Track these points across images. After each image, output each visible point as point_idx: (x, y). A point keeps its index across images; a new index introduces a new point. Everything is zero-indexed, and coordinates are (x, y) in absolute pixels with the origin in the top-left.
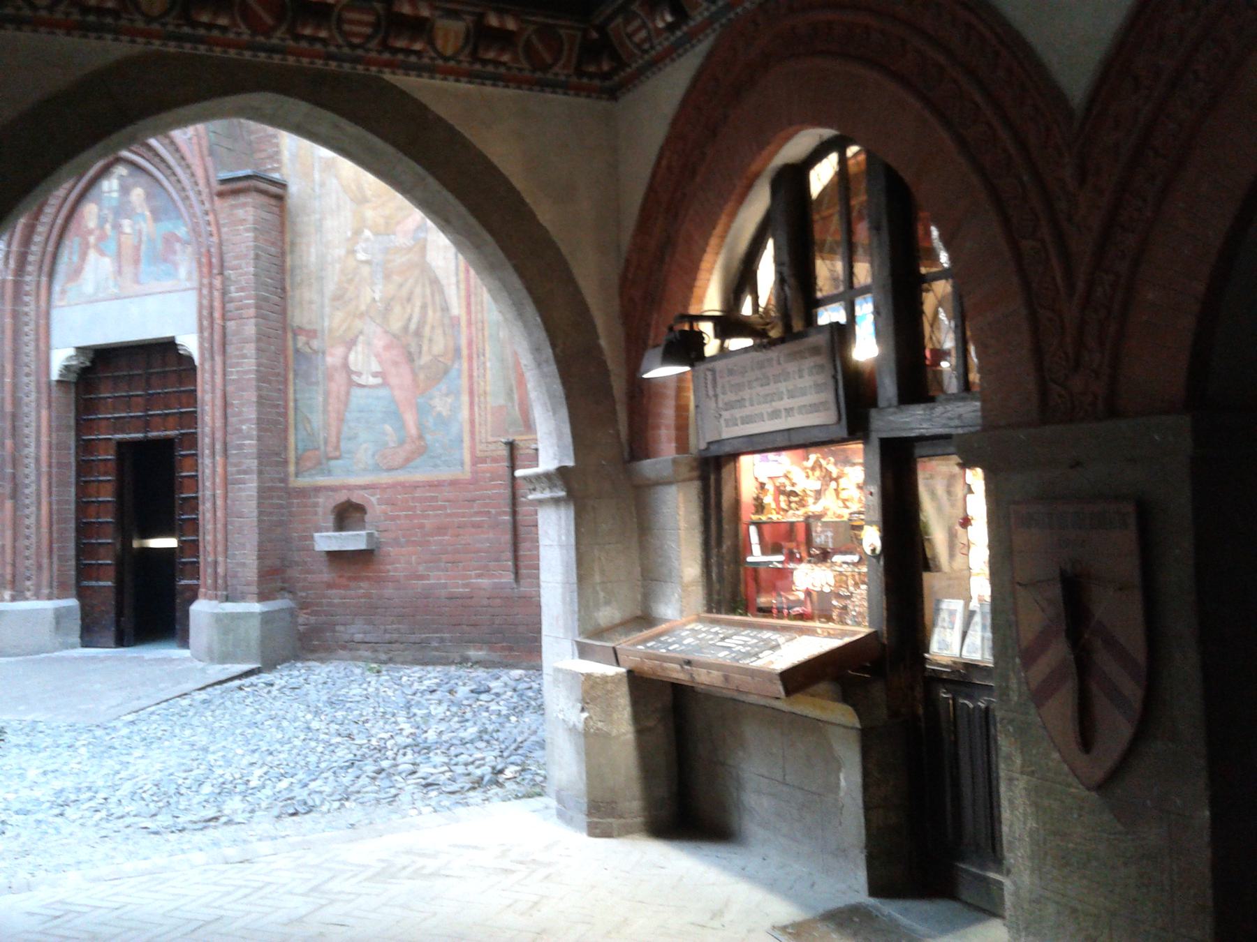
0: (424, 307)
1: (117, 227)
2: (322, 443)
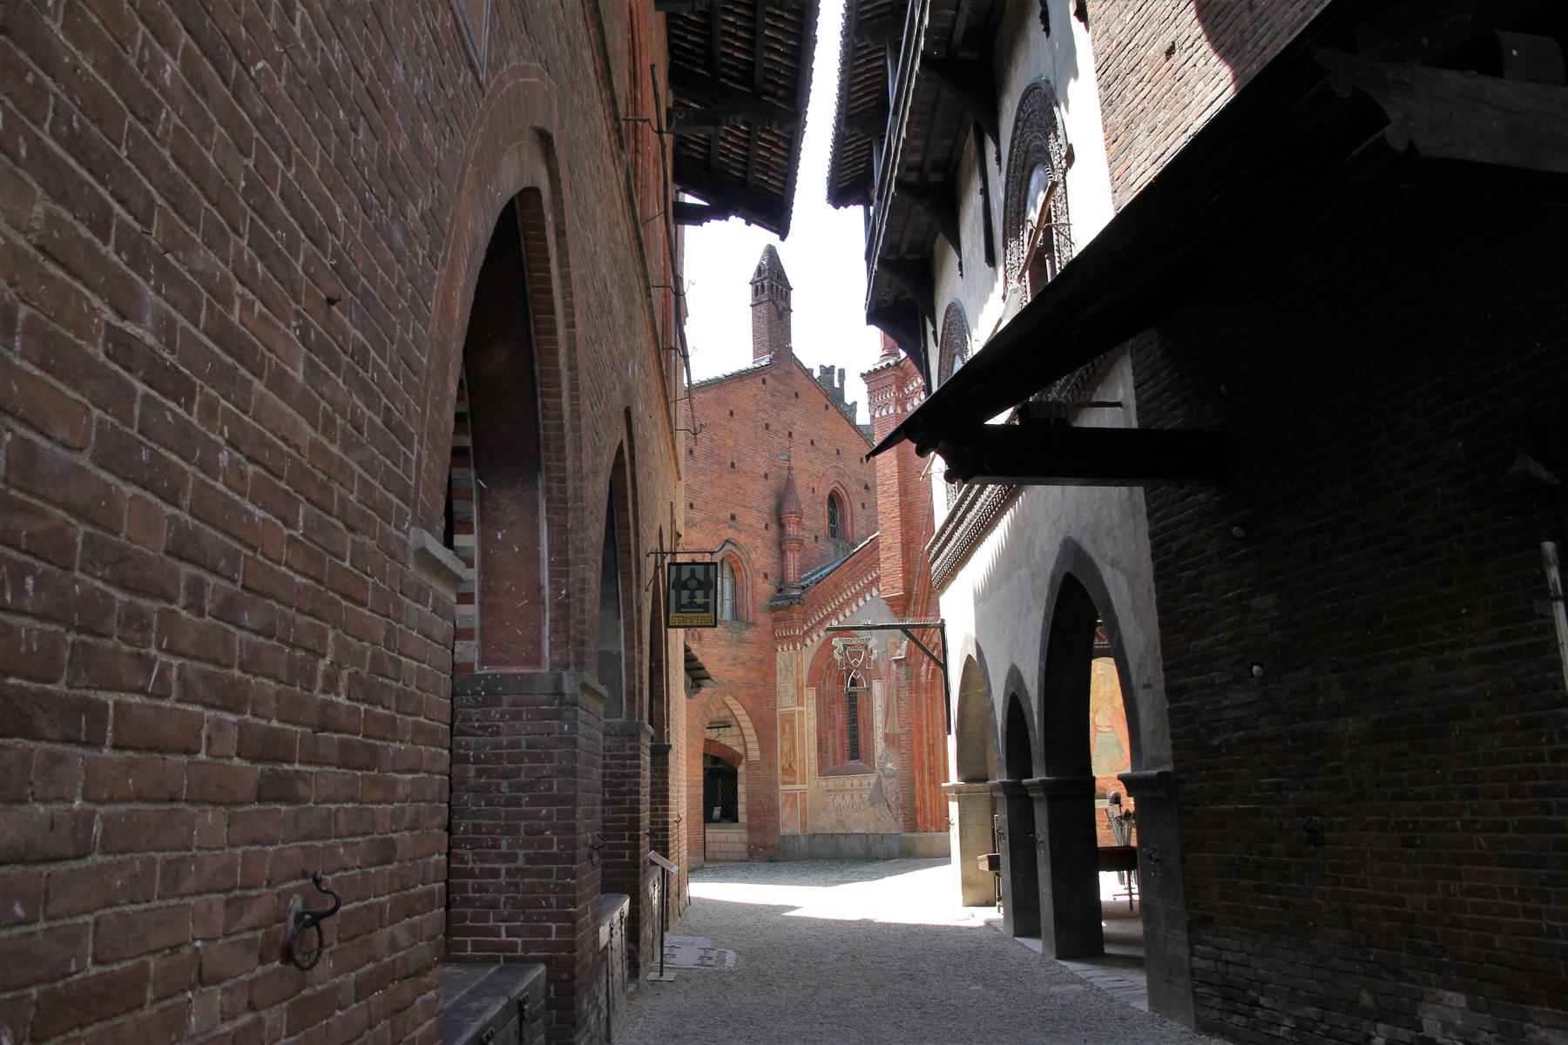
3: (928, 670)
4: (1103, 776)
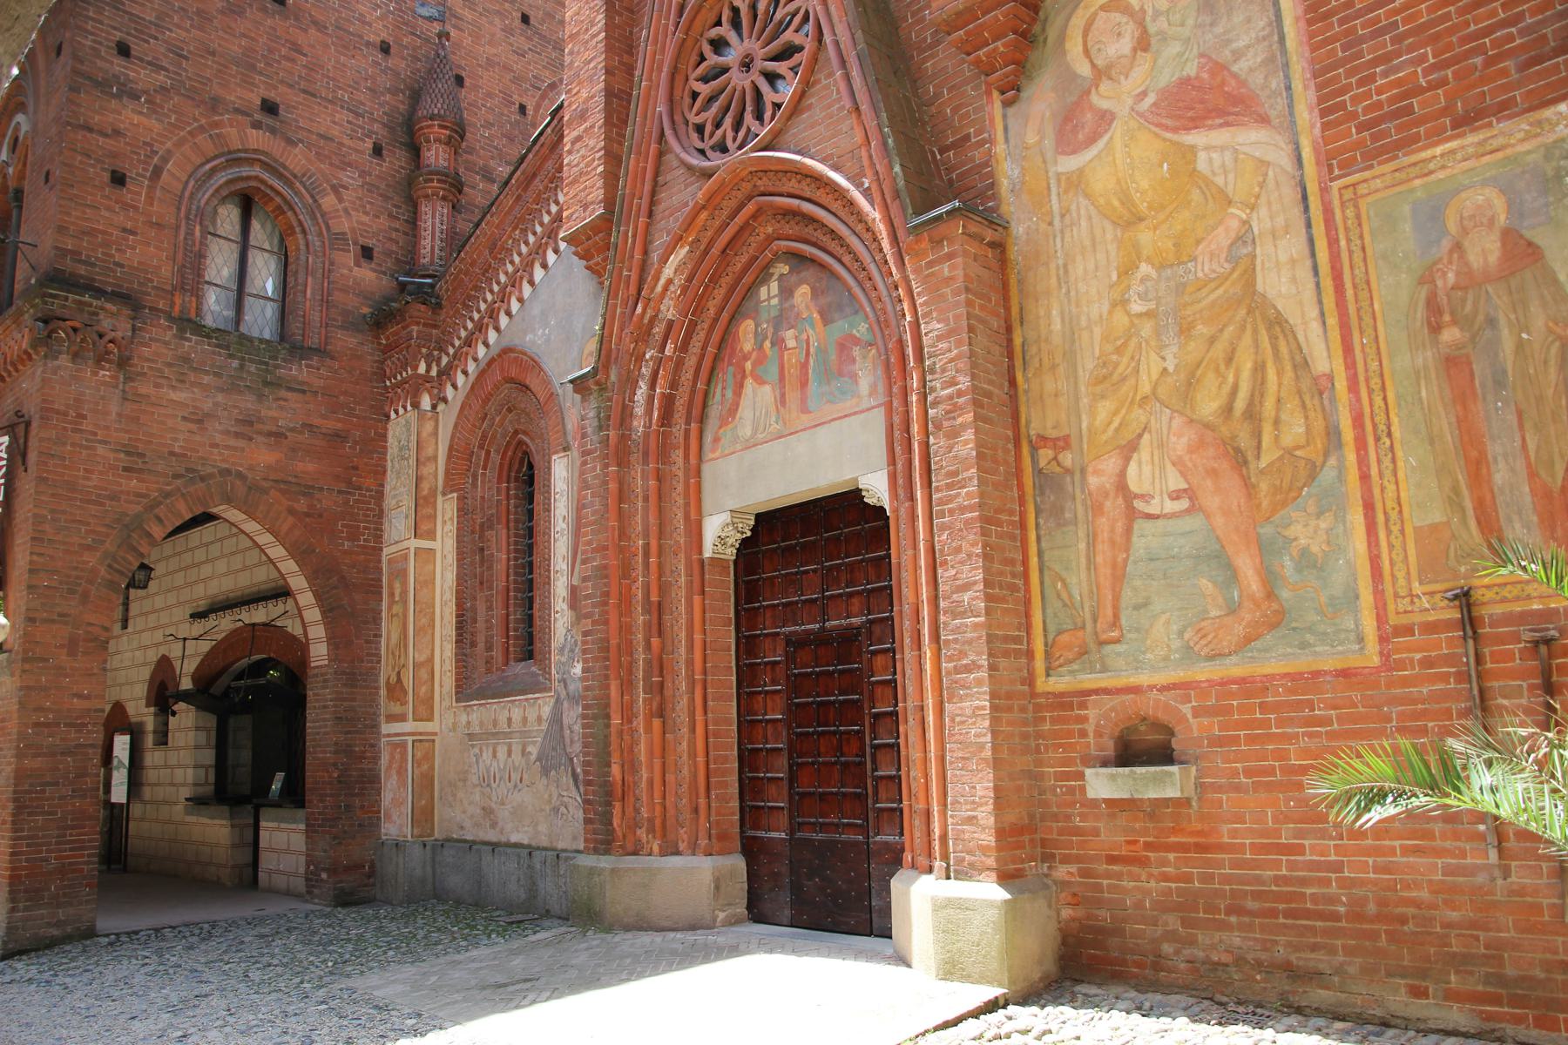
0: (1259, 368)
1: (778, 342)
2: (1088, 616)
3: (650, 399)
4: (1161, 678)
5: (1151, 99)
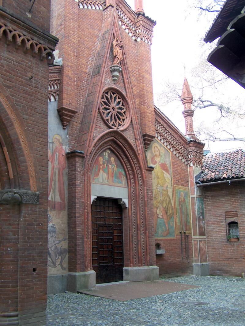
5: (160, 163)
